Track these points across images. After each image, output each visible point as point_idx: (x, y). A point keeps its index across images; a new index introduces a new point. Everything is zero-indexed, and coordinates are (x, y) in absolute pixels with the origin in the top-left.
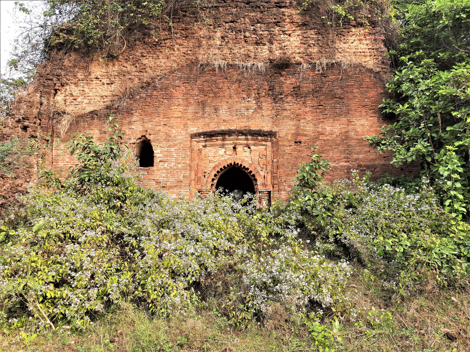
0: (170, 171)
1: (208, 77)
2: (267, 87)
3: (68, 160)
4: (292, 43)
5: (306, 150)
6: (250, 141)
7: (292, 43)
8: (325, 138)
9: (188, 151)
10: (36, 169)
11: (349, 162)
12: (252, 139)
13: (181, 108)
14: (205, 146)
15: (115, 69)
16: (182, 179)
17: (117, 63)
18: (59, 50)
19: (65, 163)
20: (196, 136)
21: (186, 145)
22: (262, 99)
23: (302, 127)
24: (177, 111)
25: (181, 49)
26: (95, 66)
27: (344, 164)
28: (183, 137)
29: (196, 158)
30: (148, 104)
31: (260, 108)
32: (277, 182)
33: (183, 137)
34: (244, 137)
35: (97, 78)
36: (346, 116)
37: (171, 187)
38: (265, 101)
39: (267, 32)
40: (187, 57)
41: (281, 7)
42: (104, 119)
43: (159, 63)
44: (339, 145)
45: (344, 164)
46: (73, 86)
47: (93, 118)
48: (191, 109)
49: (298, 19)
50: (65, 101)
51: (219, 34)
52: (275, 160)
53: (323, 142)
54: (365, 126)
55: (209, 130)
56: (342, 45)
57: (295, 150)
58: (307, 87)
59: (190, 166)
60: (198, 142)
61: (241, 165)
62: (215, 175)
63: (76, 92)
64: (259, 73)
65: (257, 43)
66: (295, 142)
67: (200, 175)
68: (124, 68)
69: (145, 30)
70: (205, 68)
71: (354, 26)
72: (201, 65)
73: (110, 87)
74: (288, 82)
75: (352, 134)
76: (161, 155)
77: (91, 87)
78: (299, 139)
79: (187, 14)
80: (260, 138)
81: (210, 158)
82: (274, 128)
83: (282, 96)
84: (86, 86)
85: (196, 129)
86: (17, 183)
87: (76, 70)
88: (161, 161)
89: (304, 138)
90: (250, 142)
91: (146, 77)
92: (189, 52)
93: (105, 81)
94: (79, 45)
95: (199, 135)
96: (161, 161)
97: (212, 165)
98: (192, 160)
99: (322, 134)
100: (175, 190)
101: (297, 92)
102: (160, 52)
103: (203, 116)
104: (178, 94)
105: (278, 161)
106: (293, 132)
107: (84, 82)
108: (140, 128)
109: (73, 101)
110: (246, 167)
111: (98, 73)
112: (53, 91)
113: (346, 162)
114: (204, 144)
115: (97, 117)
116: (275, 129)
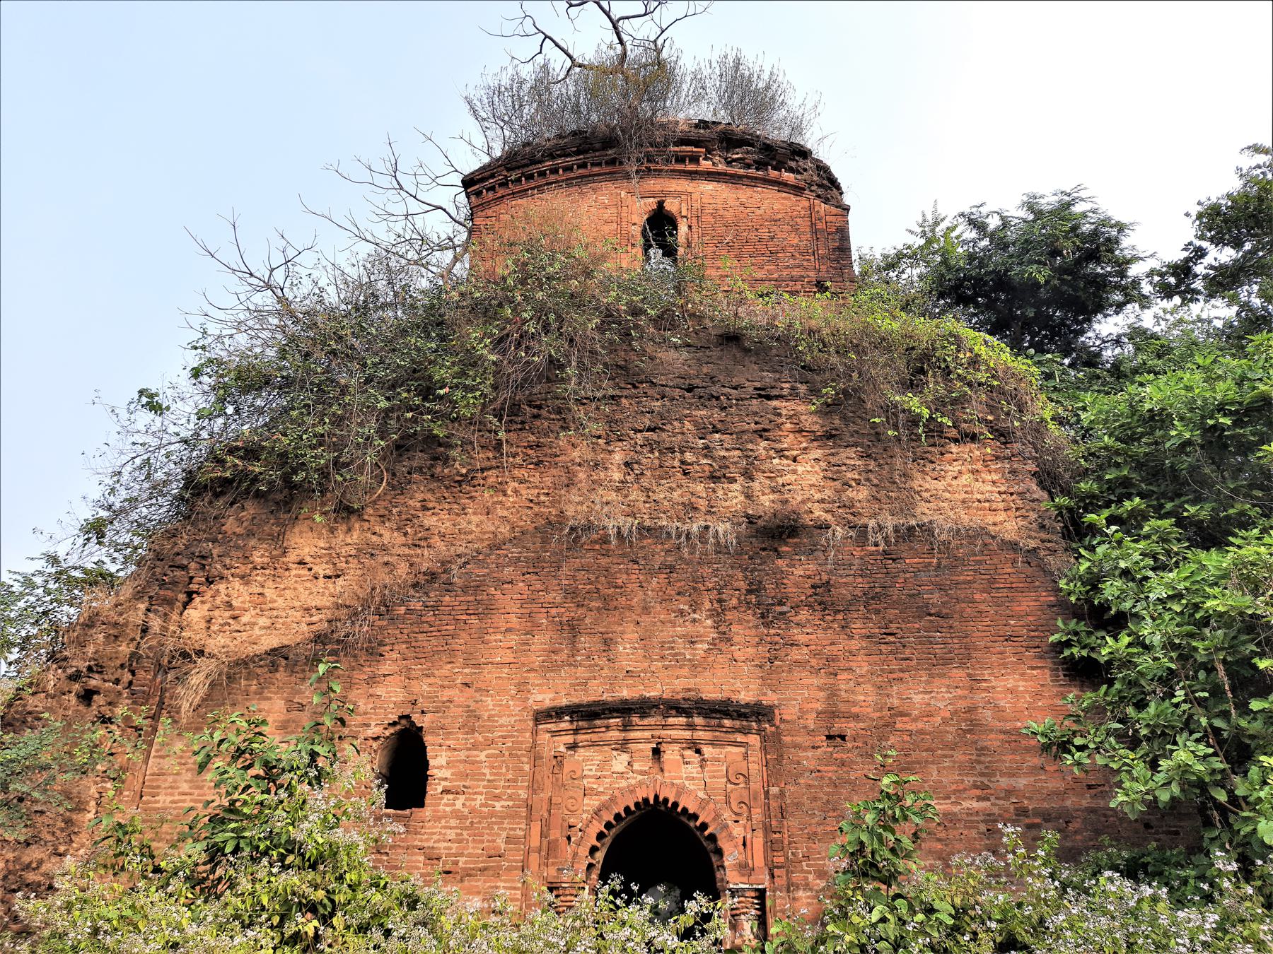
0: (471, 823)
1: (589, 559)
2: (743, 585)
3: (185, 787)
4: (803, 478)
5: (859, 759)
6: (701, 733)
7: (803, 478)
8: (912, 727)
9: (525, 759)
10: (91, 815)
11: (988, 799)
12: (707, 727)
13: (513, 639)
14: (573, 747)
15: (351, 538)
16: (503, 846)
17: (357, 526)
18: (217, 495)
19: (177, 798)
20: (551, 717)
21: (522, 742)
22: (729, 616)
23: (843, 693)
24: (501, 646)
25: (524, 492)
26: (301, 532)
27: (975, 805)
28: (513, 719)
29: (548, 783)
30: (426, 627)
31: (725, 638)
32: (782, 859)
33: (513, 719)
34: (682, 720)
35: (301, 563)
36: (962, 665)
37: (468, 874)
38: (740, 622)
39: (737, 453)
40: (536, 509)
41: (769, 398)
42: (303, 671)
43: (464, 525)
44: (952, 747)
45: (975, 805)
46: (237, 583)
47: (274, 667)
48: (540, 642)
49: (811, 422)
50: (209, 621)
51: (618, 457)
53: (906, 738)
54: (1022, 694)
56: (930, 484)
57: (829, 760)
58: (849, 584)
59: (530, 808)
60: (555, 733)
61: (676, 804)
62: (600, 836)
63: (240, 599)
64: (720, 549)
65: (714, 478)
66: (829, 737)
67: (556, 834)
68: (374, 538)
69: (436, 448)
70: (582, 536)
71: (956, 441)
72: (572, 529)
73: (331, 586)
74: (798, 571)
75: (987, 715)
76: (447, 773)
77: (282, 586)
78: (838, 727)
79: (544, 412)
80: (727, 722)
81: (585, 781)
82: (765, 694)
83: (785, 609)
84: (270, 583)
85: (551, 696)
86: (26, 859)
87: (252, 542)
88: (446, 791)
89: (851, 725)
90: (701, 734)
91: (427, 560)
92: (543, 498)
93: (322, 569)
94: (271, 484)
95: (557, 713)
96: (446, 791)
97: (592, 803)
98: (534, 788)
99: (902, 714)
100: (480, 883)
101: (823, 598)
102: (471, 498)
103: (571, 660)
104: (509, 602)
105: (782, 793)
106: (819, 706)
107: (267, 572)
109: (231, 621)
110: (691, 811)
111: (307, 550)
112: (182, 597)
113: (979, 799)
115: (287, 665)
116: (769, 698)
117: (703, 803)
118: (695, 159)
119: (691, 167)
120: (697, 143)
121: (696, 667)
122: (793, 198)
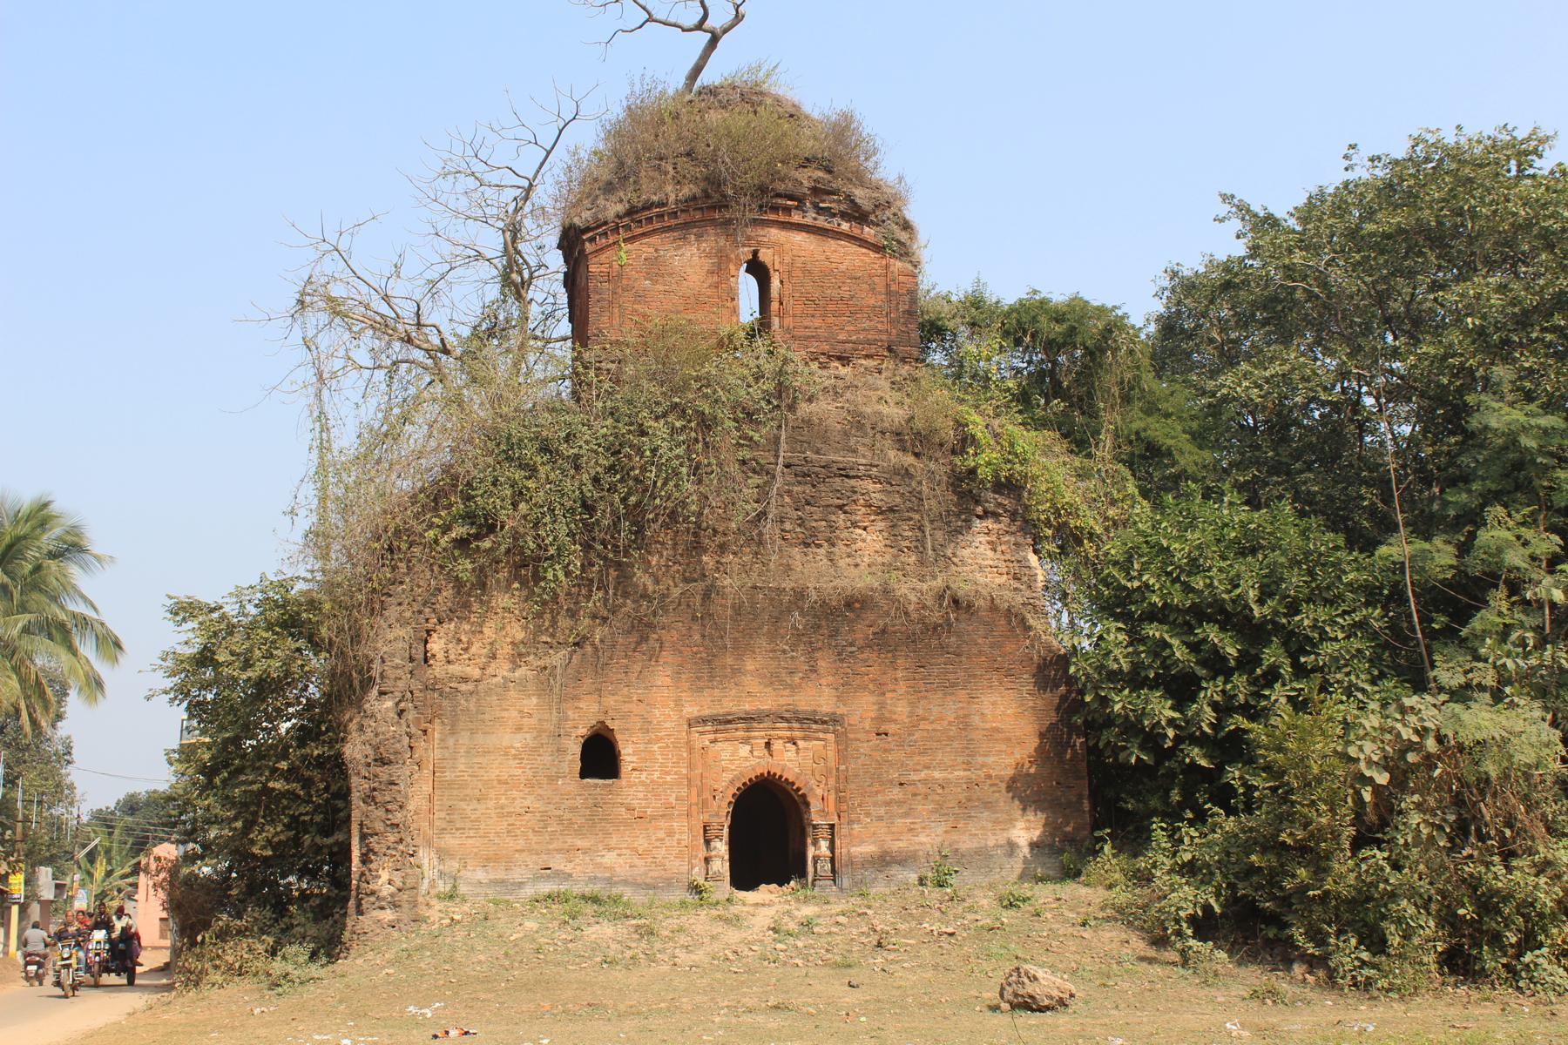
3: (462, 767)
37: (654, 818)
44: (951, 739)
52: (843, 767)
55: (721, 711)
57: (876, 748)
67: (707, 795)
71: (979, 517)
75: (976, 720)
76: (634, 759)
90: (797, 734)
97: (727, 776)
98: (691, 767)
99: (924, 719)
100: (662, 823)
106: (873, 715)
108: (595, 708)
114: (712, 737)
116: (842, 710)
117: (798, 776)
118: (787, 210)
119: (782, 219)
120: (791, 198)
121: (793, 688)
122: (872, 254)
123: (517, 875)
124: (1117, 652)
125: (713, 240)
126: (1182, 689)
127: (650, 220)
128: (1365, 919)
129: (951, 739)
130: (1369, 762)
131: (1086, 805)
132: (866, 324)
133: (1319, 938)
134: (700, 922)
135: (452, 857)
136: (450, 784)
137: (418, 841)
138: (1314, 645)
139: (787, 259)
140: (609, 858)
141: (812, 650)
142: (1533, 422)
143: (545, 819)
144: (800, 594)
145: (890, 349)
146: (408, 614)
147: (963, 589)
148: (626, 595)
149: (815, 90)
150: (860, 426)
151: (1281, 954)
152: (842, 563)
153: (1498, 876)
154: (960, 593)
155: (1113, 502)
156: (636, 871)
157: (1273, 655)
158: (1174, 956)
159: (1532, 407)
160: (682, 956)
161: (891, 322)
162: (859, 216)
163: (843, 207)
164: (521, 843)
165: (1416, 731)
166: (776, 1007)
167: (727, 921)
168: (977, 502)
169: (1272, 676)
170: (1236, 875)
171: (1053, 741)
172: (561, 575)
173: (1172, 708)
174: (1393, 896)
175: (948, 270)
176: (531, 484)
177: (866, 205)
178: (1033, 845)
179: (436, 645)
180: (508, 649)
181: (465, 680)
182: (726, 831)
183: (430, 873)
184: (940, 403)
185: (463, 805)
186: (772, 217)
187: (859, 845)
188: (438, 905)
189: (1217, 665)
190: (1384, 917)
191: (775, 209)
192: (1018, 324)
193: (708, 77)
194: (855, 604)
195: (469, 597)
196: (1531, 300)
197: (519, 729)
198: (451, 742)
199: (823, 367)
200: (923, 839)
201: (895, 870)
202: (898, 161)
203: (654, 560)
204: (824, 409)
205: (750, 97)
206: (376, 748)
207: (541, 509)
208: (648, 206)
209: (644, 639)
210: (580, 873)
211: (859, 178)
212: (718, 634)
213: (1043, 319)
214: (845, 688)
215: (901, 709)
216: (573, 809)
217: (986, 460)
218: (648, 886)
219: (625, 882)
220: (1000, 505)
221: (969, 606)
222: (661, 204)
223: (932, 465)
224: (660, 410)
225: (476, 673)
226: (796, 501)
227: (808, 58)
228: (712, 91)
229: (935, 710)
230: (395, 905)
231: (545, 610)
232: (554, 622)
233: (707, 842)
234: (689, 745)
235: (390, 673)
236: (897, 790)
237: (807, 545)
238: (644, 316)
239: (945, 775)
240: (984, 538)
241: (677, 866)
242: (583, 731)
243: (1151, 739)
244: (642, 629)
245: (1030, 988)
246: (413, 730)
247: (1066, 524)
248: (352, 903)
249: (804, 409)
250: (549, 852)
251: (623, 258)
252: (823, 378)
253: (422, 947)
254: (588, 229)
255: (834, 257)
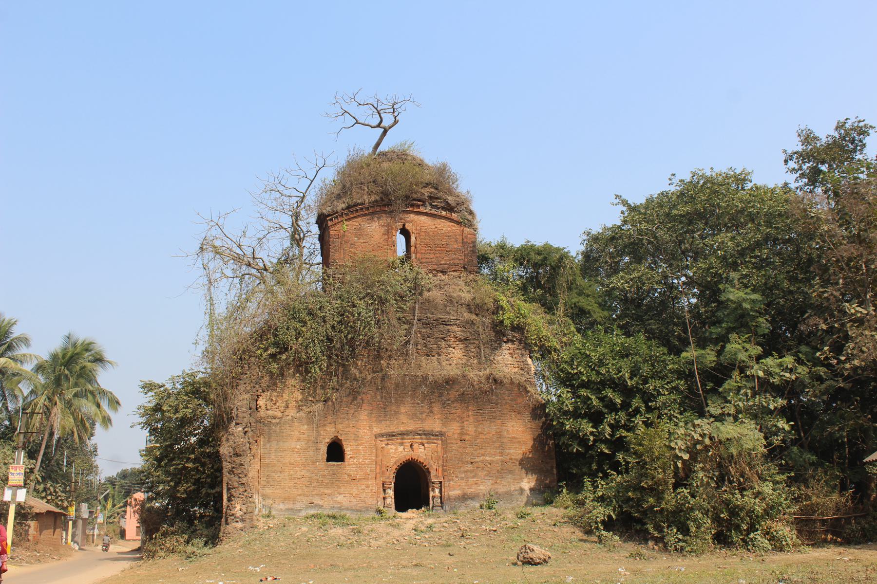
31: (431, 412)
37: (360, 480)
44: (494, 442)
57: (460, 447)
67: (384, 469)
75: (505, 433)
78: (463, 438)
95: (382, 435)
97: (393, 460)
98: (376, 456)
100: (364, 482)
117: (425, 460)
118: (418, 206)
119: (416, 210)
120: (420, 201)
121: (422, 420)
123: (298, 506)
124: (567, 402)
125: (385, 220)
126: (596, 418)
127: (357, 211)
128: (679, 519)
129: (494, 442)
130: (680, 450)
131: (555, 471)
132: (454, 257)
133: (659, 529)
134: (381, 526)
135: (269, 498)
136: (268, 465)
137: (253, 491)
138: (655, 398)
139: (418, 228)
140: (340, 498)
141: (431, 403)
142: (748, 297)
143: (311, 481)
144: (425, 378)
145: (464, 268)
146: (249, 388)
147: (498, 375)
148: (347, 379)
149: (430, 153)
150: (451, 302)
151: (643, 537)
152: (444, 364)
153: (738, 499)
154: (497, 376)
155: (565, 335)
156: (352, 504)
157: (636, 402)
158: (595, 539)
159: (748, 290)
160: (373, 542)
161: (465, 255)
162: (450, 208)
163: (443, 205)
164: (300, 492)
165: (700, 435)
166: (416, 565)
167: (394, 526)
168: (504, 336)
169: (637, 411)
170: (622, 502)
171: (539, 442)
172: (318, 370)
173: (592, 427)
174: (692, 509)
175: (488, 233)
176: (304, 329)
177: (453, 204)
178: (531, 490)
179: (261, 402)
180: (294, 404)
181: (274, 418)
182: (393, 485)
183: (259, 505)
184: (487, 291)
185: (273, 474)
186: (411, 209)
187: (453, 491)
188: (262, 520)
189: (612, 407)
190: (688, 519)
191: (412, 206)
192: (523, 256)
193: (383, 148)
194: (450, 382)
195: (276, 380)
196: (745, 244)
197: (299, 440)
198: (268, 446)
199: (435, 276)
200: (482, 487)
201: (469, 502)
202: (467, 184)
203: (359, 363)
204: (435, 294)
205: (401, 156)
206: (234, 449)
207: (308, 341)
208: (356, 205)
209: (355, 399)
210: (327, 505)
211: (450, 192)
212: (389, 396)
213: (532, 253)
214: (446, 420)
215: (471, 429)
216: (324, 476)
217: (508, 317)
218: (358, 511)
219: (347, 509)
220: (514, 337)
221: (501, 382)
222: (362, 204)
223: (484, 319)
224: (362, 296)
225: (279, 414)
226: (423, 336)
227: (428, 141)
228: (384, 154)
229: (486, 429)
230: (243, 520)
231: (310, 385)
232: (315, 391)
233: (384, 490)
234: (376, 445)
235: (240, 415)
236: (470, 465)
237: (428, 356)
238: (355, 253)
239: (491, 458)
240: (507, 352)
241: (371, 501)
242: (328, 440)
243: (583, 441)
244: (354, 394)
245: (531, 555)
246: (251, 441)
247: (544, 345)
248: (223, 520)
249: (426, 294)
250: (313, 496)
251: (345, 227)
252: (435, 280)
253: (255, 539)
254: (329, 215)
255: (439, 227)
